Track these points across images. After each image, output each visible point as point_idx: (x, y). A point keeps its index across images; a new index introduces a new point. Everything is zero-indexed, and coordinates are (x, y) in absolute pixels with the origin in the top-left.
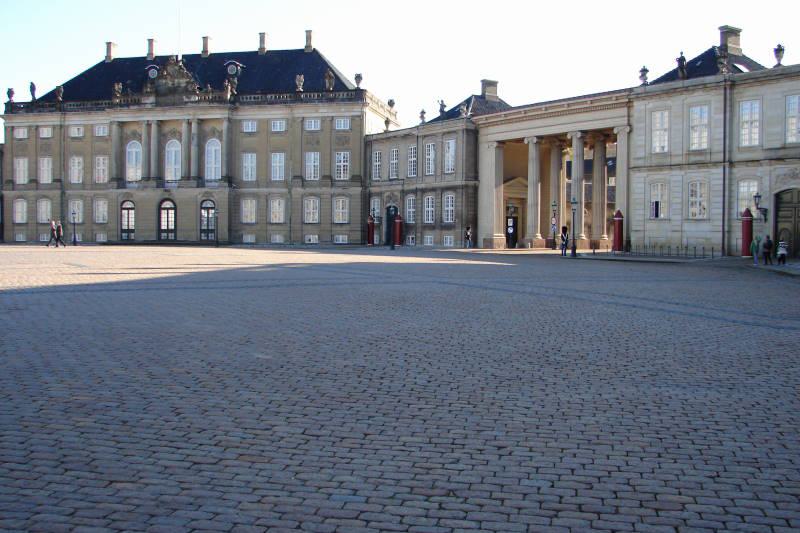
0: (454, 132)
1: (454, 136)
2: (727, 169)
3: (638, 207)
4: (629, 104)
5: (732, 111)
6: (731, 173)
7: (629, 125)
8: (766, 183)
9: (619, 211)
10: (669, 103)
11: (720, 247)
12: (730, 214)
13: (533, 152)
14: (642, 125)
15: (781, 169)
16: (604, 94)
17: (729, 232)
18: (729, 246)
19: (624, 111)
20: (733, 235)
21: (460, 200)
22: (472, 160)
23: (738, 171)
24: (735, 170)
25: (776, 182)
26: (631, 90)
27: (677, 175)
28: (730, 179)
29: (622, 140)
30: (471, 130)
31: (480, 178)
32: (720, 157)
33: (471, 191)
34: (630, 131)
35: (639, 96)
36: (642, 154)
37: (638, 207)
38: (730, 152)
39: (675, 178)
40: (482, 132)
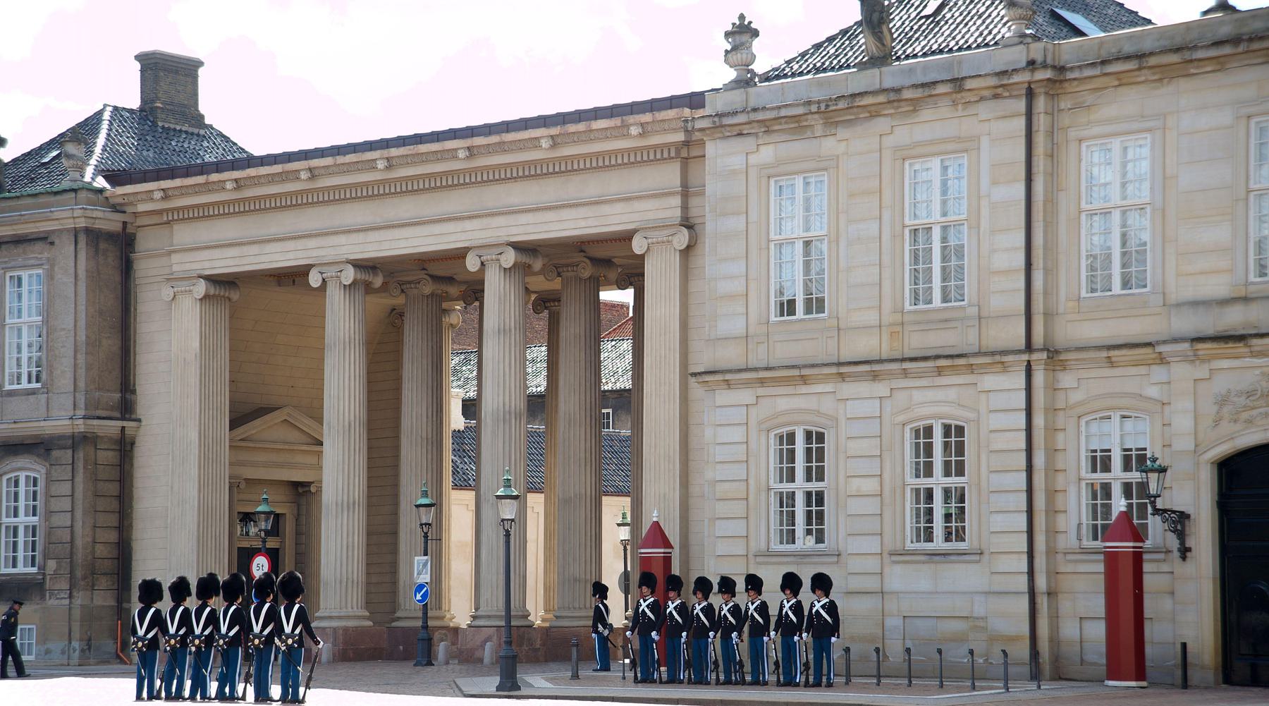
0: (44, 239)
1: (38, 252)
2: (1039, 378)
3: (722, 509)
4: (687, 153)
5: (1052, 175)
6: (1052, 389)
7: (688, 224)
8: (1183, 422)
9: (656, 525)
10: (830, 145)
11: (1023, 651)
12: (1052, 532)
13: (342, 322)
14: (737, 223)
16: (597, 113)
17: (1051, 594)
18: (1055, 641)
19: (670, 175)
20: (1065, 605)
21: (65, 488)
22: (111, 344)
23: (1079, 385)
24: (1067, 380)
25: (1217, 422)
26: (695, 100)
28: (1052, 410)
29: (661, 274)
30: (110, 236)
31: (140, 411)
32: (1015, 334)
33: (107, 456)
34: (687, 252)
35: (724, 126)
36: (738, 327)
37: (722, 509)
38: (1048, 315)
39: (854, 409)
40: (146, 242)
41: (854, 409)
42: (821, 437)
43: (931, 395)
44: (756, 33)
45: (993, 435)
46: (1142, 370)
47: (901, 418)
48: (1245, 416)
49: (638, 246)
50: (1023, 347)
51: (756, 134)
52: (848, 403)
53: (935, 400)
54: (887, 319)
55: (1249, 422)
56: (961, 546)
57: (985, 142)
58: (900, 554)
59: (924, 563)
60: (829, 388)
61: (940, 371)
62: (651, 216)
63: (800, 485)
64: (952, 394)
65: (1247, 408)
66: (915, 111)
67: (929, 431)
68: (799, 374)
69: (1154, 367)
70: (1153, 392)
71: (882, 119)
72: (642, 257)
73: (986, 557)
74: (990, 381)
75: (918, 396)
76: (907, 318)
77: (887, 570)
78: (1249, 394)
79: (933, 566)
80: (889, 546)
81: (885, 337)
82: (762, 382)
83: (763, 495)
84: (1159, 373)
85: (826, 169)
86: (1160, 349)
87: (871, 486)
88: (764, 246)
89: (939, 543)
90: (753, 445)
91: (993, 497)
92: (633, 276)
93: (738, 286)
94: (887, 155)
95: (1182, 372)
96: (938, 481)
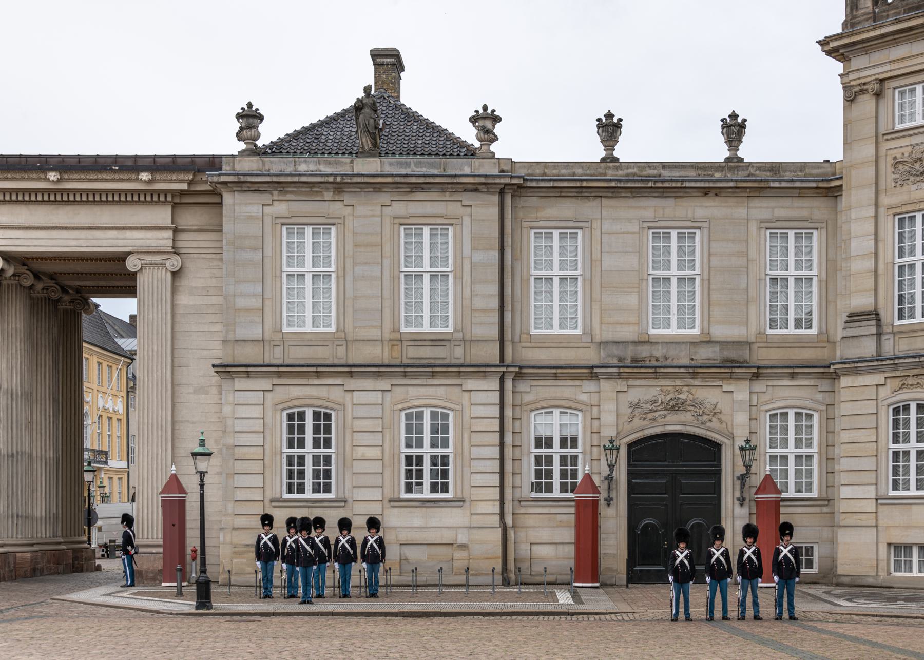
2: (509, 384)
10: (336, 208)
15: (646, 391)
23: (532, 391)
24: (523, 386)
25: (631, 418)
27: (367, 393)
32: (491, 353)
36: (255, 332)
41: (359, 397)
42: (328, 417)
43: (422, 390)
44: (261, 118)
45: (473, 421)
46: (577, 383)
47: (399, 407)
48: (650, 416)
49: (132, 264)
50: (498, 363)
51: (271, 192)
52: (355, 393)
53: (425, 395)
54: (387, 335)
55: (654, 420)
56: (449, 495)
57: (466, 221)
58: (395, 501)
59: (416, 507)
60: (338, 381)
61: (433, 375)
62: (149, 243)
63: (309, 450)
64: (441, 391)
65: (652, 411)
66: (411, 192)
67: (420, 416)
68: (316, 371)
69: (586, 383)
70: (584, 397)
71: (383, 194)
72: (135, 274)
73: (467, 504)
74: (471, 384)
75: (412, 391)
76: (403, 337)
77: (386, 512)
78: (654, 402)
79: (424, 509)
80: (389, 495)
81: (386, 349)
82: (279, 375)
83: (278, 457)
84: (590, 386)
85: (334, 224)
86: (595, 370)
87: (375, 453)
88: (278, 274)
89: (427, 494)
90: (269, 419)
91: (474, 463)
92: (126, 286)
93: (257, 303)
94: (387, 222)
95: (606, 386)
96: (427, 451)
